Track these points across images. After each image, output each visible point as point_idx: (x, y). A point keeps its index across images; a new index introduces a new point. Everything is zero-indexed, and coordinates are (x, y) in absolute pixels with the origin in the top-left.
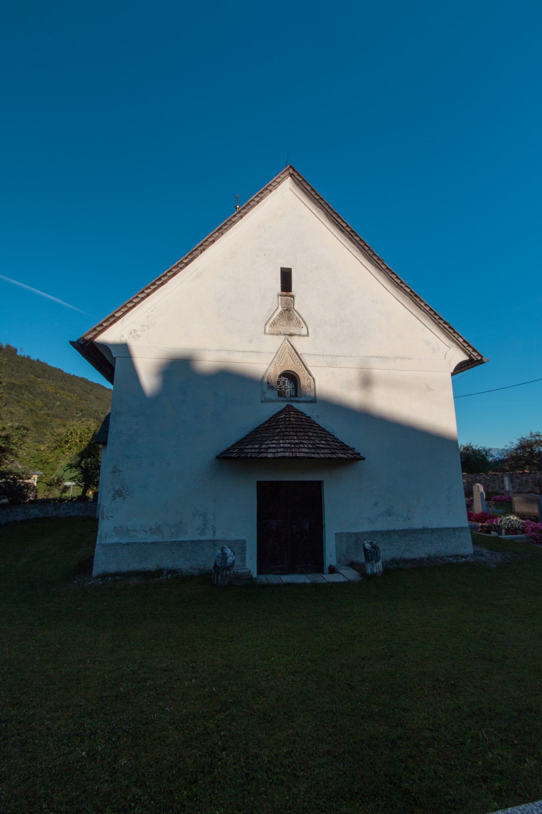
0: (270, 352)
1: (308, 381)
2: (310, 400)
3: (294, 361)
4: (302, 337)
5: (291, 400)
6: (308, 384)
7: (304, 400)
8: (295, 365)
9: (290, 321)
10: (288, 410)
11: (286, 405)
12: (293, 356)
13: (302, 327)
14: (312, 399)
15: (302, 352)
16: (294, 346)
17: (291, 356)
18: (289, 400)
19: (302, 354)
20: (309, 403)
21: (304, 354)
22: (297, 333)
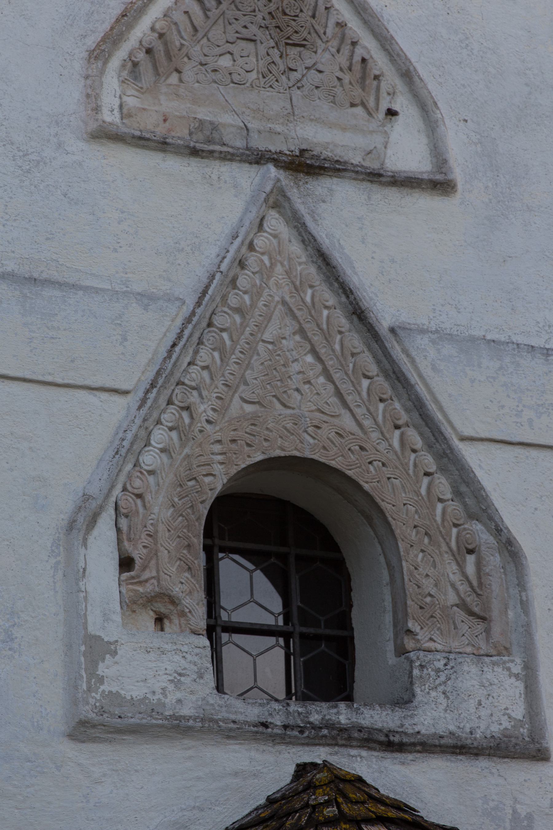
0: (138, 288)
1: (461, 566)
2: (495, 729)
3: (346, 387)
4: (393, 193)
5: (330, 725)
6: (463, 588)
7: (441, 729)
8: (348, 422)
9: (293, 52)
10: (330, 811)
11: (291, 769)
12: (328, 338)
13: (391, 113)
14: (506, 724)
15: (405, 317)
16: (337, 257)
17: (317, 339)
18: (314, 727)
19: (405, 329)
20: (483, 763)
21: (423, 331)
22: (356, 159)
